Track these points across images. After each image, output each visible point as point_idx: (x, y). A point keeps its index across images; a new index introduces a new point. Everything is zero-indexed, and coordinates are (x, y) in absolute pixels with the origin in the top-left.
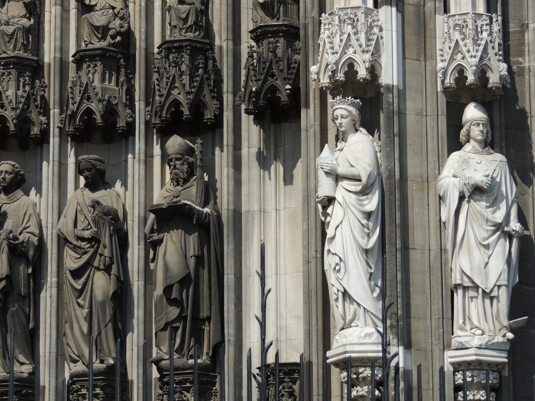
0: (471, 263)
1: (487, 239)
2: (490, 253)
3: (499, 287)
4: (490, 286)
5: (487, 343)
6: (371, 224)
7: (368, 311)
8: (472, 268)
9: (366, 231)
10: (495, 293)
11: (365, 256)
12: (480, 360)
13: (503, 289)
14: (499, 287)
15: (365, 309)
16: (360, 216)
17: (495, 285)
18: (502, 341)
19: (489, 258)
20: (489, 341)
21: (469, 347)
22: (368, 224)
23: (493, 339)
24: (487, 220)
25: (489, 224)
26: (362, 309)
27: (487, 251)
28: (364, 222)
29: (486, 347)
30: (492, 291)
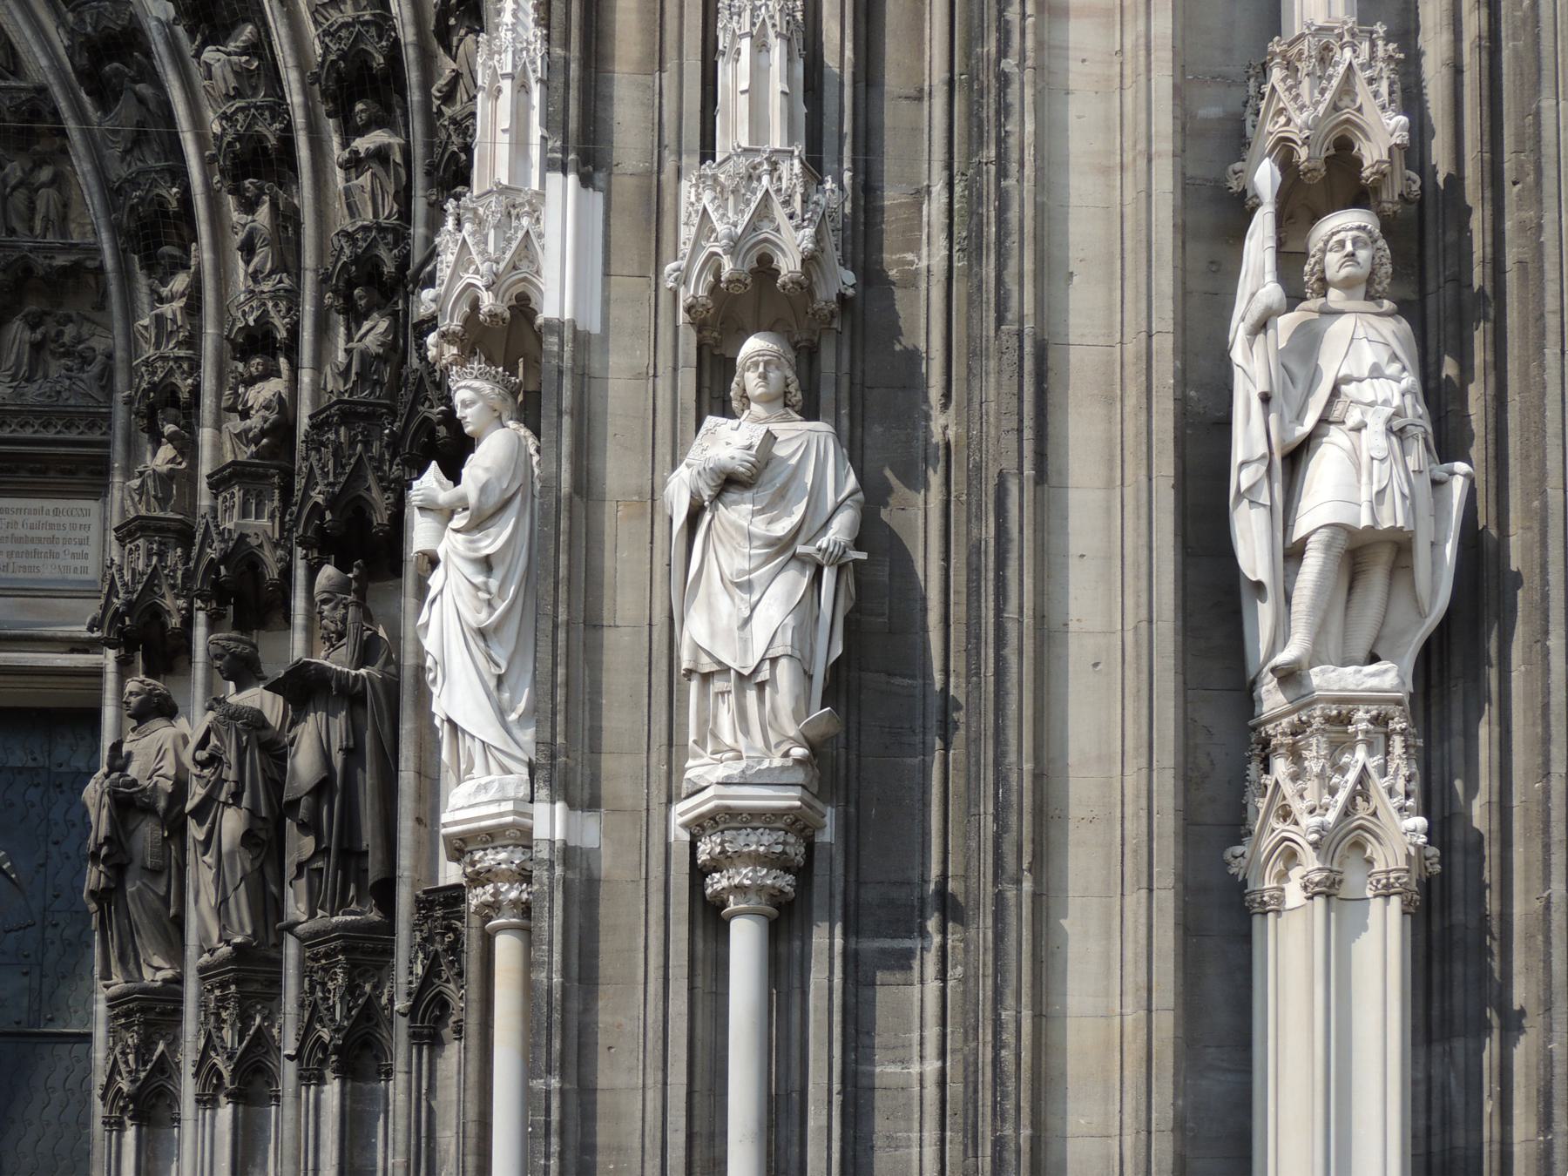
0: (712, 624)
1: (750, 572)
2: (755, 598)
3: (774, 661)
4: (752, 663)
6: (494, 583)
8: (713, 635)
9: (486, 596)
10: (765, 674)
11: (482, 645)
13: (783, 664)
14: (774, 661)
16: (469, 570)
17: (763, 660)
19: (752, 610)
22: (486, 584)
23: (759, 763)
24: (750, 537)
25: (756, 543)
26: (478, 745)
27: (747, 597)
28: (479, 579)
30: (756, 671)
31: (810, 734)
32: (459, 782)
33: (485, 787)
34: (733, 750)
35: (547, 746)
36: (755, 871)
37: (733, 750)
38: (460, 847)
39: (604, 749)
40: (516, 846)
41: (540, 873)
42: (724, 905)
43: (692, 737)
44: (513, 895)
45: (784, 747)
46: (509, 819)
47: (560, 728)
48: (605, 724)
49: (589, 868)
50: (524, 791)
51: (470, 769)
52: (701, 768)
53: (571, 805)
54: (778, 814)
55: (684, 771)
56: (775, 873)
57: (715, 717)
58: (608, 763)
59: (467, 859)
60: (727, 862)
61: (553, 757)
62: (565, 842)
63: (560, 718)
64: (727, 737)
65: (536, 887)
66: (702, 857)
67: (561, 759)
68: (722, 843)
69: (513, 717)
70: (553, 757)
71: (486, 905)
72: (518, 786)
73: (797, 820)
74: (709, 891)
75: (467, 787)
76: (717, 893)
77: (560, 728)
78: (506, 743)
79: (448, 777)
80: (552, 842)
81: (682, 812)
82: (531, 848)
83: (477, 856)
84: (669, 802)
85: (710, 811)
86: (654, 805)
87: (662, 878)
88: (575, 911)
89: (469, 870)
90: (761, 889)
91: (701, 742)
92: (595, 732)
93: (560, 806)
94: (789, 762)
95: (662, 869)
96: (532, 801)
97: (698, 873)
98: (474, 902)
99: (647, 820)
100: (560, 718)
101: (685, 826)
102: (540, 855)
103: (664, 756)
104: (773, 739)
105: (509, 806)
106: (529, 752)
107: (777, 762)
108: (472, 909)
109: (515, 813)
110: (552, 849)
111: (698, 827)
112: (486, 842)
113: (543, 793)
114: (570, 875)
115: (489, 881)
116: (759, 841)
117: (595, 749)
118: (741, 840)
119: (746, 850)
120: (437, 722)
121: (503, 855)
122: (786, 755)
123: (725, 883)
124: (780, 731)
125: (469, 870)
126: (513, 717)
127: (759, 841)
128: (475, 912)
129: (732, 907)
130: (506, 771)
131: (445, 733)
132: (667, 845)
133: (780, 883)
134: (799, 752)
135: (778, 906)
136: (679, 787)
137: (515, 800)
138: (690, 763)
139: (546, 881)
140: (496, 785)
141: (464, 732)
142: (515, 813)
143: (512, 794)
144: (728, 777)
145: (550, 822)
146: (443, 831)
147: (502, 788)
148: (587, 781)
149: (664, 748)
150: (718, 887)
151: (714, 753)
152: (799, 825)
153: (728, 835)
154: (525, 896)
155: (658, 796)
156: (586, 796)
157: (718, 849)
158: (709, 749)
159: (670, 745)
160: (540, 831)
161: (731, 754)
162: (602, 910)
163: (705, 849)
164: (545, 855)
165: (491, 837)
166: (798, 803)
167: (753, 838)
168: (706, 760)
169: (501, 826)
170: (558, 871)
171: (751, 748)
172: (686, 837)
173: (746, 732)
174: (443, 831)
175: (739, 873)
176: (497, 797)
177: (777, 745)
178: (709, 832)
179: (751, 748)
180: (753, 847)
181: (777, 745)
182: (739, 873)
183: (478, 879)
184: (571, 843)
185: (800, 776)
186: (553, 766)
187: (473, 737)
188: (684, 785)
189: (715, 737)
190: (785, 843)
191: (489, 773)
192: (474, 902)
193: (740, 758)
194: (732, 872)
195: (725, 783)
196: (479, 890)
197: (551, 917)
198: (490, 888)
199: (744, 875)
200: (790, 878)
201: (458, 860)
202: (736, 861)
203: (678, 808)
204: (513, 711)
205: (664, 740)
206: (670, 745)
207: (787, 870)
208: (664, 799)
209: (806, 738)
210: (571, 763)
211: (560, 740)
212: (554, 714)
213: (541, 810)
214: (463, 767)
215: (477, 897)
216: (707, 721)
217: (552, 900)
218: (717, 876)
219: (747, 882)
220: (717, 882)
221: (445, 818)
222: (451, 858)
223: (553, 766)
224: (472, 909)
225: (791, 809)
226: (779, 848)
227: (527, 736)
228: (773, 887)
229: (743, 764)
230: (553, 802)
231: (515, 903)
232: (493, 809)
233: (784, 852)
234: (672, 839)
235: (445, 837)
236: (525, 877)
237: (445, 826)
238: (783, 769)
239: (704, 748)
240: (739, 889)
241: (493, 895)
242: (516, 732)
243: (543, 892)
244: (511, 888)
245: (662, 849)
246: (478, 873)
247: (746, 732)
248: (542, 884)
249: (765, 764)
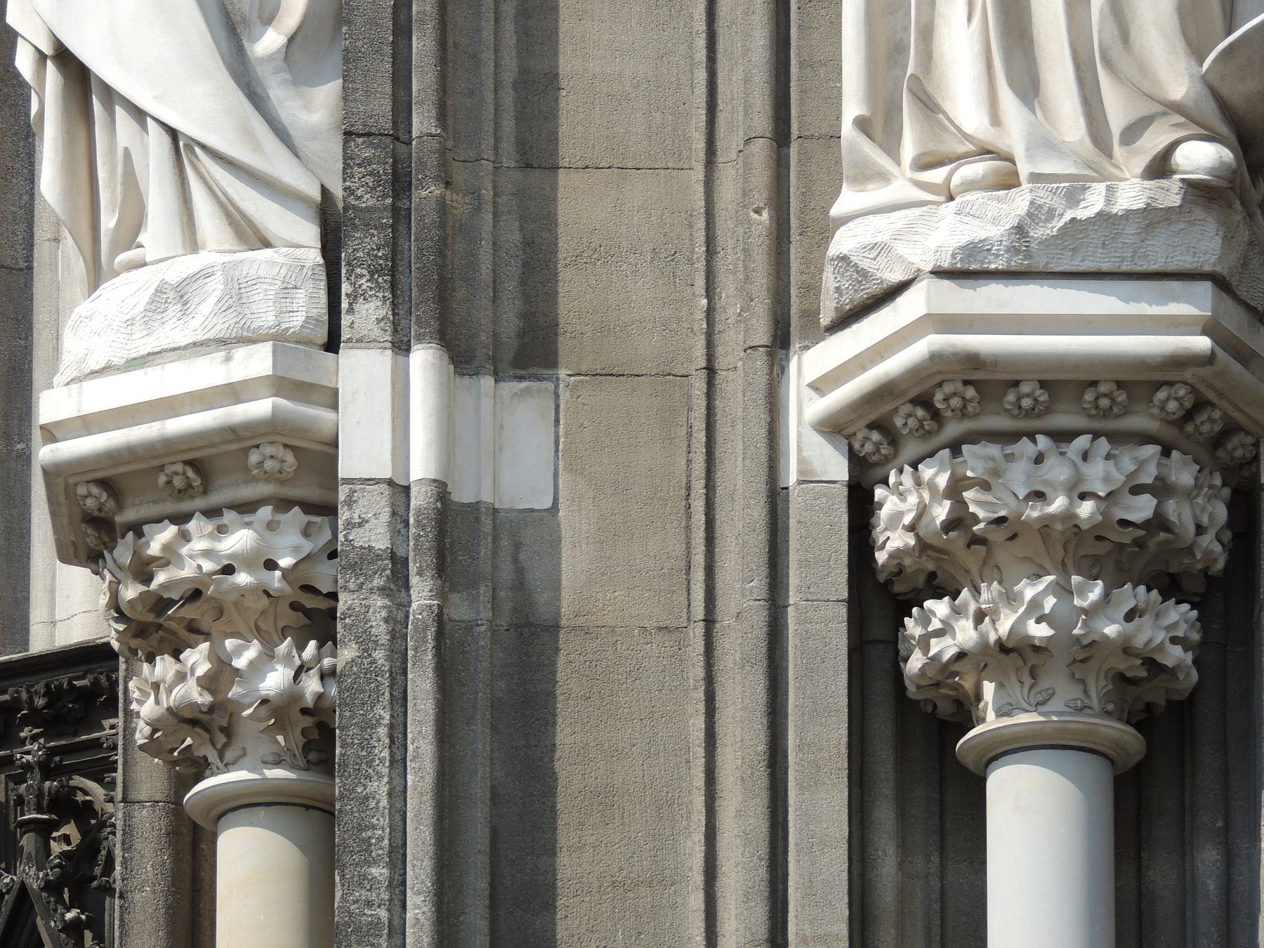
5: (1020, 230)
7: (193, 143)
12: (973, 361)
15: (173, 133)
18: (1139, 204)
20: (1035, 213)
21: (896, 277)
23: (1073, 197)
26: (157, 141)
29: (1017, 262)
31: (1239, 91)
32: (97, 276)
33: (178, 295)
34: (986, 152)
35: (376, 141)
36: (1063, 590)
37: (986, 152)
38: (104, 510)
39: (568, 152)
40: (283, 504)
41: (362, 603)
42: (965, 715)
43: (852, 107)
44: (275, 680)
45: (1154, 141)
46: (260, 408)
47: (422, 81)
48: (567, 64)
49: (520, 585)
50: (307, 305)
51: (130, 233)
52: (887, 220)
53: (462, 358)
54: (1137, 381)
55: (827, 229)
56: (1131, 595)
57: (927, 33)
58: (580, 205)
59: (123, 553)
60: (971, 559)
61: (400, 183)
62: (441, 489)
63: (422, 45)
64: (965, 104)
65: (348, 653)
66: (892, 541)
67: (426, 193)
68: (955, 491)
69: (269, 42)
70: (400, 183)
71: (187, 719)
72: (287, 289)
73: (1200, 404)
74: (915, 663)
75: (125, 293)
76: (944, 671)
77: (422, 81)
78: (248, 135)
79: (59, 261)
80: (400, 490)
81: (828, 373)
82: (328, 510)
83: (159, 539)
84: (780, 342)
85: (915, 373)
86: (730, 353)
87: (758, 618)
88: (479, 739)
89: (130, 592)
90: (1086, 653)
91: (881, 127)
92: (538, 90)
93: (423, 360)
94: (1170, 194)
95: (758, 585)
96: (332, 345)
97: (880, 601)
98: (147, 709)
99: (709, 404)
100: (422, 45)
101: (833, 427)
102: (360, 538)
103: (761, 177)
104: (1117, 114)
105: (257, 362)
106: (319, 167)
107: (1132, 194)
108: (141, 733)
109: (280, 384)
110: (399, 517)
111: (880, 431)
112: (186, 492)
113: (367, 314)
114: (460, 610)
115: (196, 632)
116: (1076, 484)
117: (537, 155)
118: (1018, 478)
119: (1034, 512)
120: (24, 62)
121: (239, 540)
122: (1160, 167)
123: (966, 634)
124: (1139, 84)
125: (130, 592)
126: (269, 42)
127: (1076, 484)
128: (152, 747)
129: (991, 722)
130: (252, 236)
131: (49, 100)
132: (776, 498)
133: (1148, 634)
134: (1201, 157)
135: (1143, 719)
136: (812, 289)
137: (279, 338)
138: (847, 200)
139: (380, 630)
140: (216, 286)
141: (110, 95)
142: (280, 384)
143: (266, 318)
144: (972, 249)
145: (393, 416)
146: (46, 453)
147: (236, 295)
148: (513, 270)
149: (761, 150)
150: (944, 648)
151: (925, 163)
152: (1207, 424)
153: (976, 460)
154: (312, 685)
155: (745, 325)
156: (510, 322)
157: (941, 512)
158: (909, 150)
159: (781, 135)
160: (362, 454)
161: (977, 169)
162: (566, 735)
163: (908, 507)
164: (376, 536)
165: (196, 474)
166: (1202, 343)
167: (1057, 471)
168: (900, 188)
169: (232, 433)
170: (422, 593)
171: (1045, 143)
172: (837, 468)
173: (1029, 87)
174: (46, 453)
175: (1011, 598)
176: (220, 328)
177: (1132, 133)
178: (911, 449)
179: (1045, 143)
180: (1058, 504)
181: (1132, 133)
182: (1011, 598)
183: (159, 625)
184: (462, 495)
185: (1205, 244)
186: (400, 216)
187: (140, 115)
188: (829, 280)
189: (929, 106)
190: (1161, 489)
191: (192, 243)
192: (147, 709)
193: (1008, 181)
194: (990, 592)
195: (963, 271)
196: (164, 667)
197: (399, 762)
198: (198, 658)
199: (1025, 605)
200: (1179, 615)
201: (93, 559)
202: (1002, 555)
203: (812, 361)
204: (268, 19)
205: (762, 121)
206: (781, 135)
207: (1171, 586)
208: (761, 334)
209: (1225, 108)
210: (460, 205)
211: (422, 122)
212: (402, 31)
213: (362, 372)
214: (108, 222)
215: (159, 689)
216: (899, 50)
217: (400, 700)
218: (939, 608)
219: (1040, 631)
220: (943, 632)
221: (52, 405)
222: (71, 553)
223: (400, 216)
224: (141, 733)
225: (1178, 362)
226: (1142, 508)
227: (315, 108)
228: (1126, 648)
229: (1018, 202)
230: (401, 347)
231: (279, 710)
232: (208, 372)
233: (1159, 523)
234: (792, 477)
235: (53, 473)
236: (315, 618)
237: (51, 433)
238: (1151, 217)
239: (891, 147)
240: (1013, 654)
241: (209, 683)
242: (279, 93)
243: (371, 672)
244: (268, 655)
245: (759, 513)
246: (160, 604)
247: (1029, 87)
248: (366, 642)
249: (1093, 203)
